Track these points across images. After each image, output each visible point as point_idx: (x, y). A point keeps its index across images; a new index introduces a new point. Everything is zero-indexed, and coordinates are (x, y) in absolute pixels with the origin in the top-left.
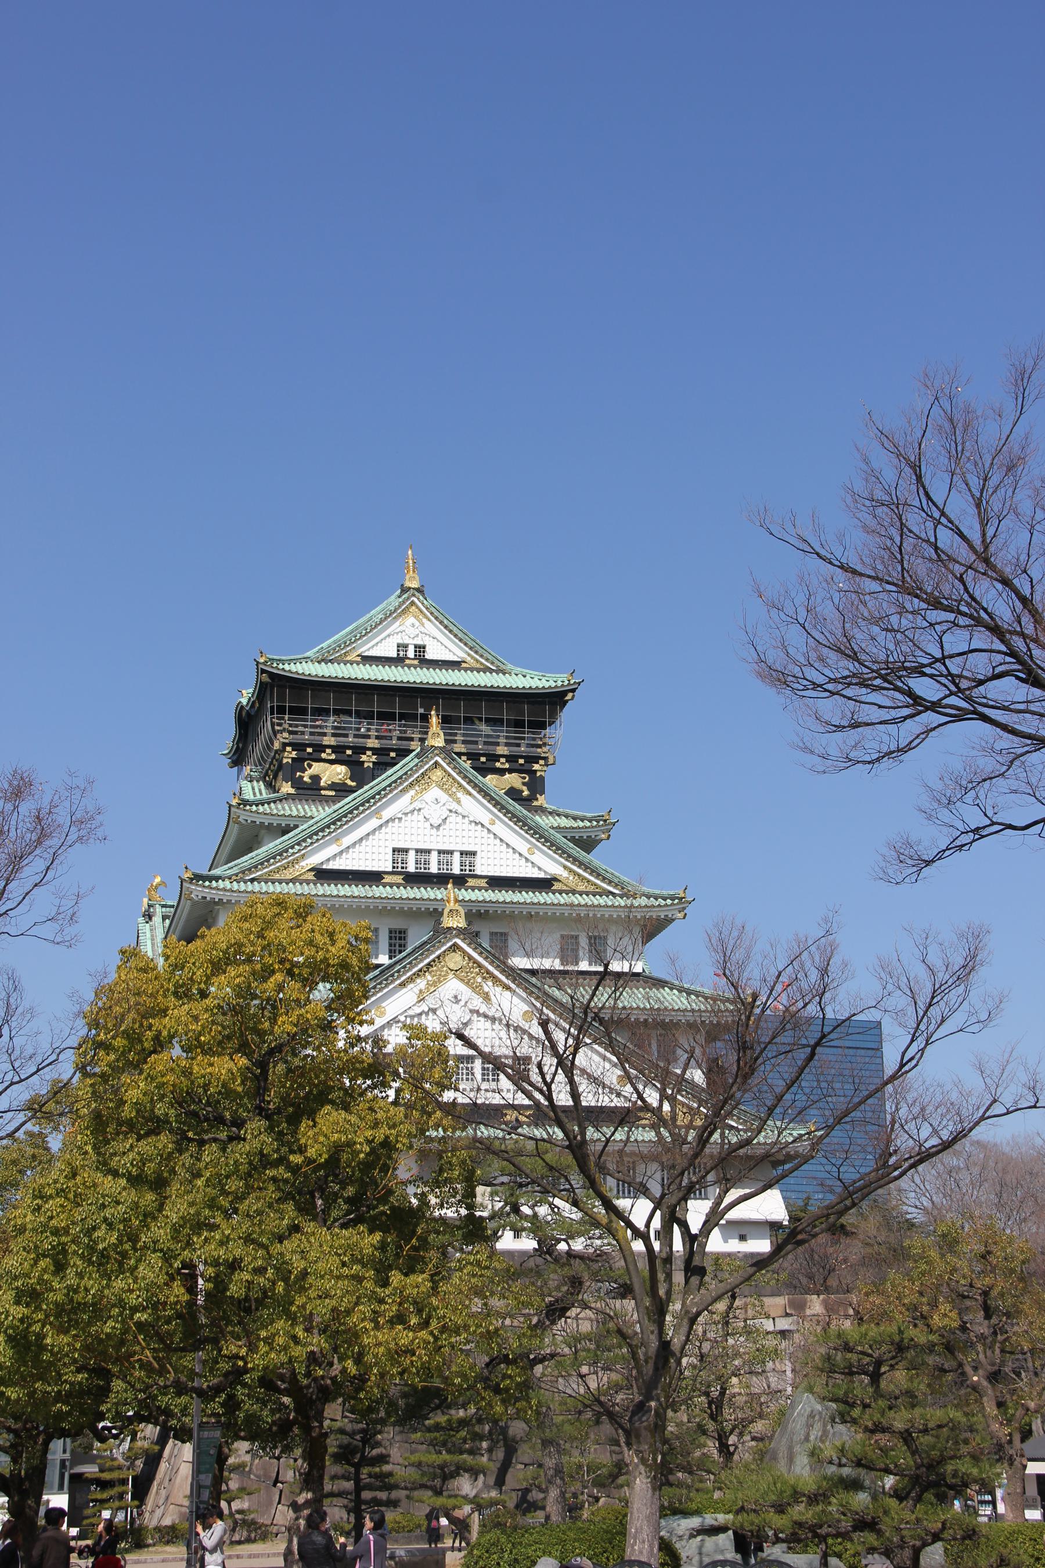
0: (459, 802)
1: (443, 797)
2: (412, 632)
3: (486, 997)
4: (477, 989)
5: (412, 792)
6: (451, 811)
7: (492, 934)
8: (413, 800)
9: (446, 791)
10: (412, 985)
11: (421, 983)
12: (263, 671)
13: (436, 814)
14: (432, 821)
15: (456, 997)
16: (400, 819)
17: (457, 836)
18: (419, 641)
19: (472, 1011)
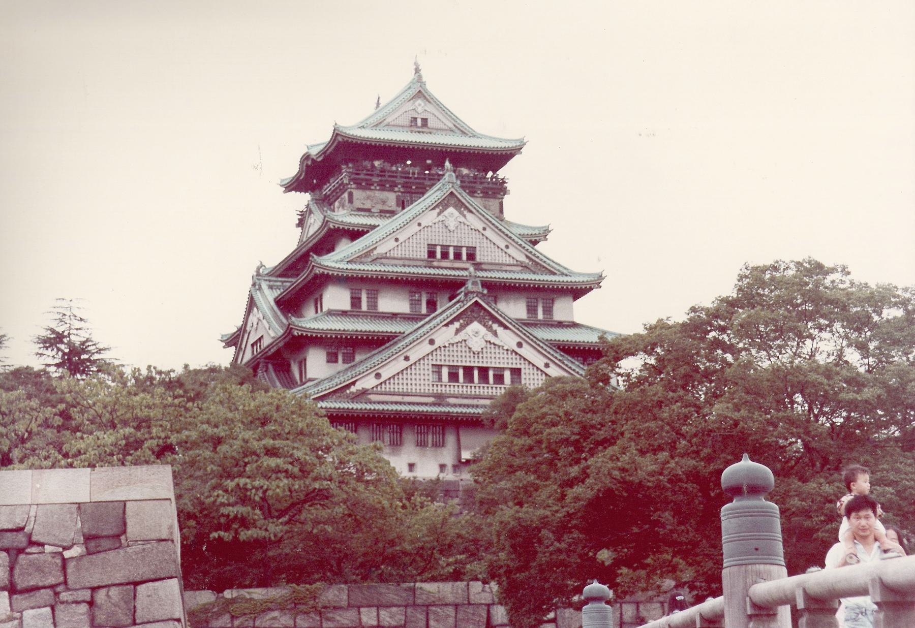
0: (465, 216)
1: (456, 213)
2: (420, 110)
3: (495, 334)
4: (489, 328)
8: (439, 214)
11: (457, 325)
12: (337, 134)
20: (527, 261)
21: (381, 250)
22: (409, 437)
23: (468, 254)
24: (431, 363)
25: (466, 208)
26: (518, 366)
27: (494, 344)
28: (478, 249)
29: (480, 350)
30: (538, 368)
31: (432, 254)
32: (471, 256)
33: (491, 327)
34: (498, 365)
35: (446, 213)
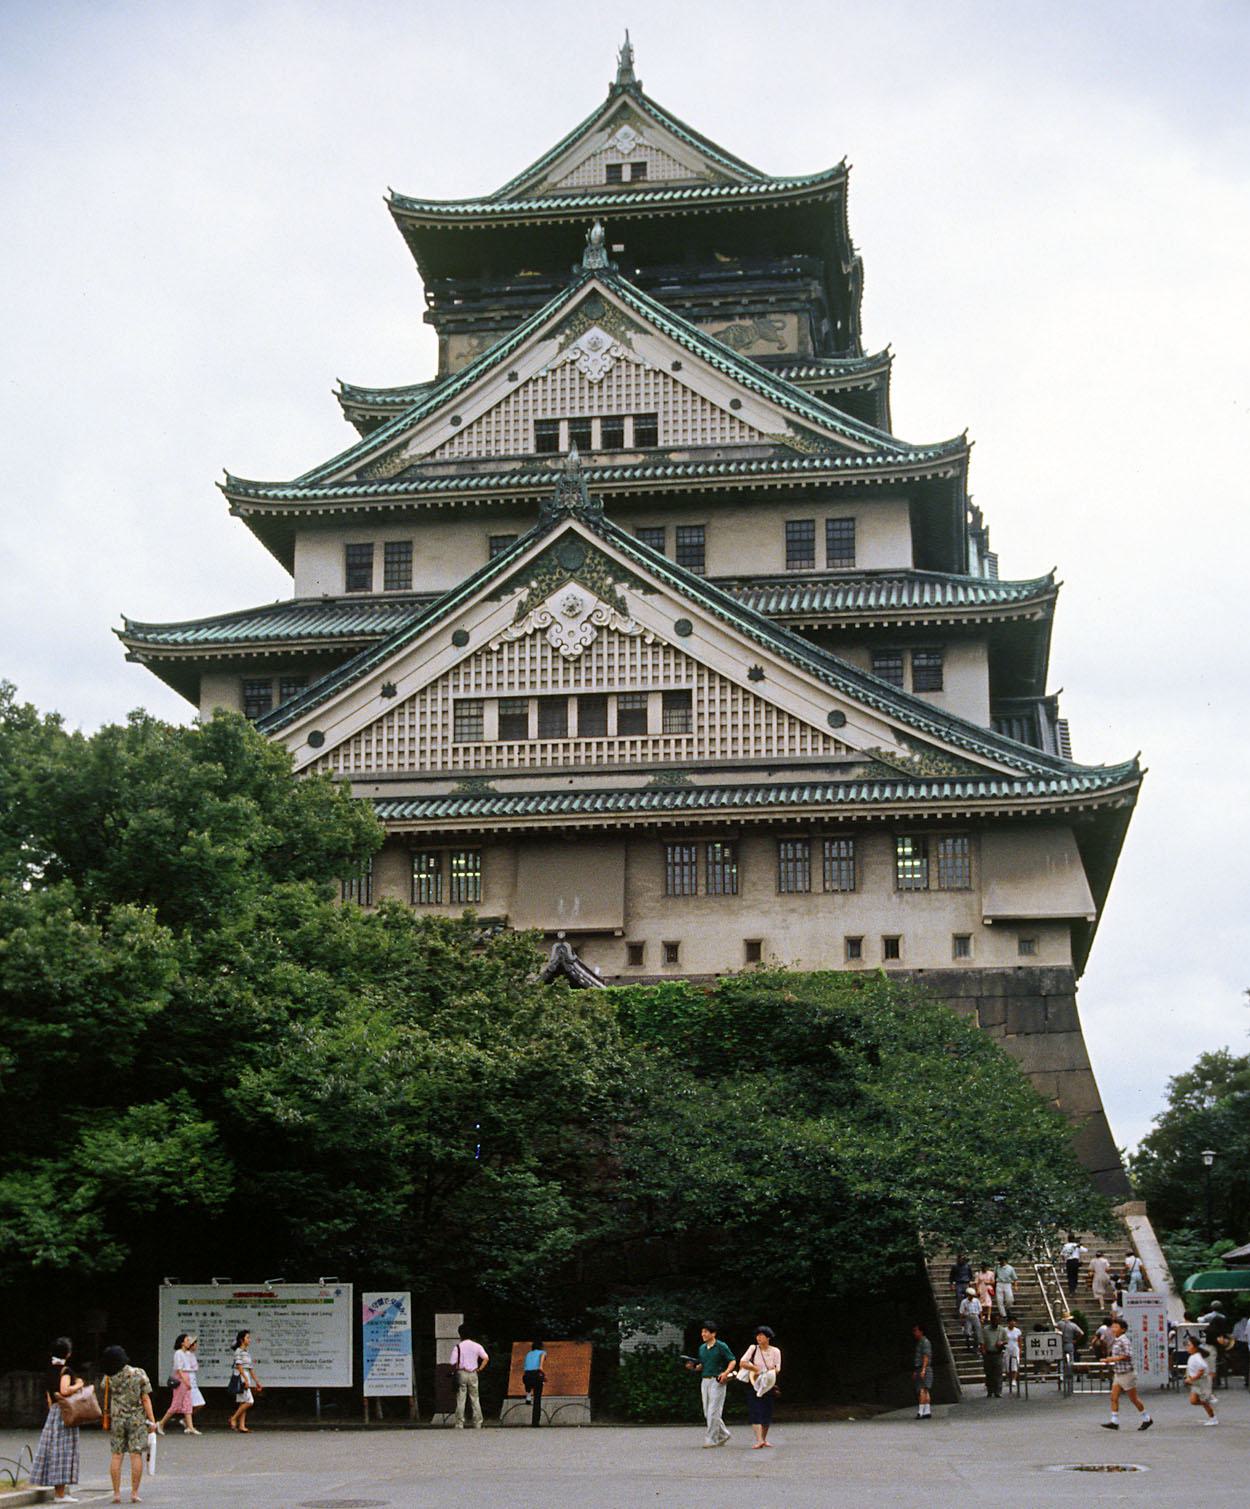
0: (629, 344)
2: (626, 146)
3: (621, 607)
5: (561, 339)
6: (618, 359)
7: (678, 528)
8: (562, 348)
9: (611, 332)
10: (510, 597)
11: (522, 594)
13: (594, 366)
14: (589, 376)
15: (571, 608)
16: (544, 379)
17: (630, 400)
18: (638, 160)
19: (599, 629)
20: (790, 433)
21: (420, 447)
22: (760, 873)
24: (452, 695)
26: (683, 685)
27: (621, 635)
29: (580, 650)
30: (735, 686)
31: (547, 441)
32: (647, 435)
33: (612, 590)
34: (628, 687)
35: (583, 342)
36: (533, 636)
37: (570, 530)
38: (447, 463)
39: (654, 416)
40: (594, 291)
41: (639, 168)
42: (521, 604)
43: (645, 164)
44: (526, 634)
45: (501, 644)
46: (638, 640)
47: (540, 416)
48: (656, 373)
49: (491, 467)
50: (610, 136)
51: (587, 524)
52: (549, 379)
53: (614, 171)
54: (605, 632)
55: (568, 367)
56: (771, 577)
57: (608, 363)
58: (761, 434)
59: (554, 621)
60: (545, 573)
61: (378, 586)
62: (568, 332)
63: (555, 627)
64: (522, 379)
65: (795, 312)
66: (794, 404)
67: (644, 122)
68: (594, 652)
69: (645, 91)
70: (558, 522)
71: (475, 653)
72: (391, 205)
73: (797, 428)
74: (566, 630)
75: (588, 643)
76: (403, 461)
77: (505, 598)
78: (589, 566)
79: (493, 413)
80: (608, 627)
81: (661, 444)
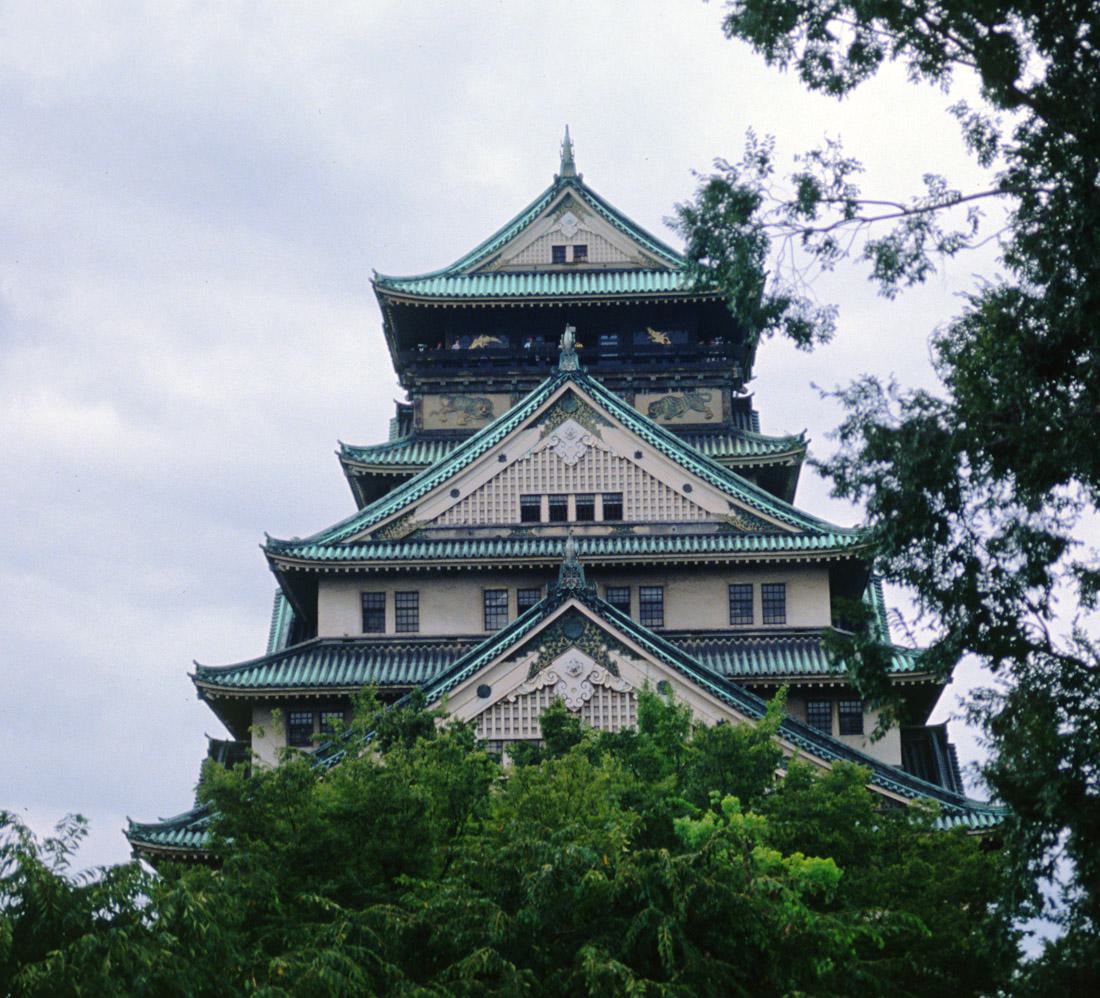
0: (598, 434)
2: (569, 231)
3: (614, 670)
4: (604, 661)
5: (541, 428)
6: (589, 447)
8: (543, 436)
9: (584, 424)
10: (523, 659)
11: (533, 657)
13: (571, 452)
14: (565, 460)
15: (574, 670)
16: (528, 461)
17: (599, 482)
18: (579, 243)
19: (596, 686)
20: (732, 513)
21: (424, 515)
23: (606, 508)
25: (600, 418)
27: (613, 691)
28: (625, 497)
29: (581, 704)
31: (530, 512)
32: (613, 511)
33: (605, 656)
36: (543, 691)
37: (572, 607)
38: (448, 529)
39: (621, 494)
40: (569, 391)
41: (581, 250)
42: (533, 665)
43: (585, 247)
44: (537, 689)
45: (517, 697)
46: (627, 697)
47: (525, 492)
48: (621, 459)
49: (484, 533)
50: (556, 221)
51: (585, 601)
52: (532, 461)
53: (559, 251)
54: (600, 689)
55: (547, 451)
56: (718, 631)
57: (582, 450)
58: (708, 513)
59: (560, 680)
60: (552, 641)
61: (390, 629)
62: (547, 422)
63: (561, 685)
64: (510, 461)
65: (720, 387)
66: (735, 490)
67: (585, 211)
68: (592, 705)
69: (586, 181)
70: (561, 602)
71: (496, 704)
72: (375, 285)
73: (738, 509)
74: (570, 686)
75: (587, 698)
76: (411, 525)
77: (520, 660)
78: (587, 635)
79: (486, 488)
80: (603, 686)
81: (626, 518)
